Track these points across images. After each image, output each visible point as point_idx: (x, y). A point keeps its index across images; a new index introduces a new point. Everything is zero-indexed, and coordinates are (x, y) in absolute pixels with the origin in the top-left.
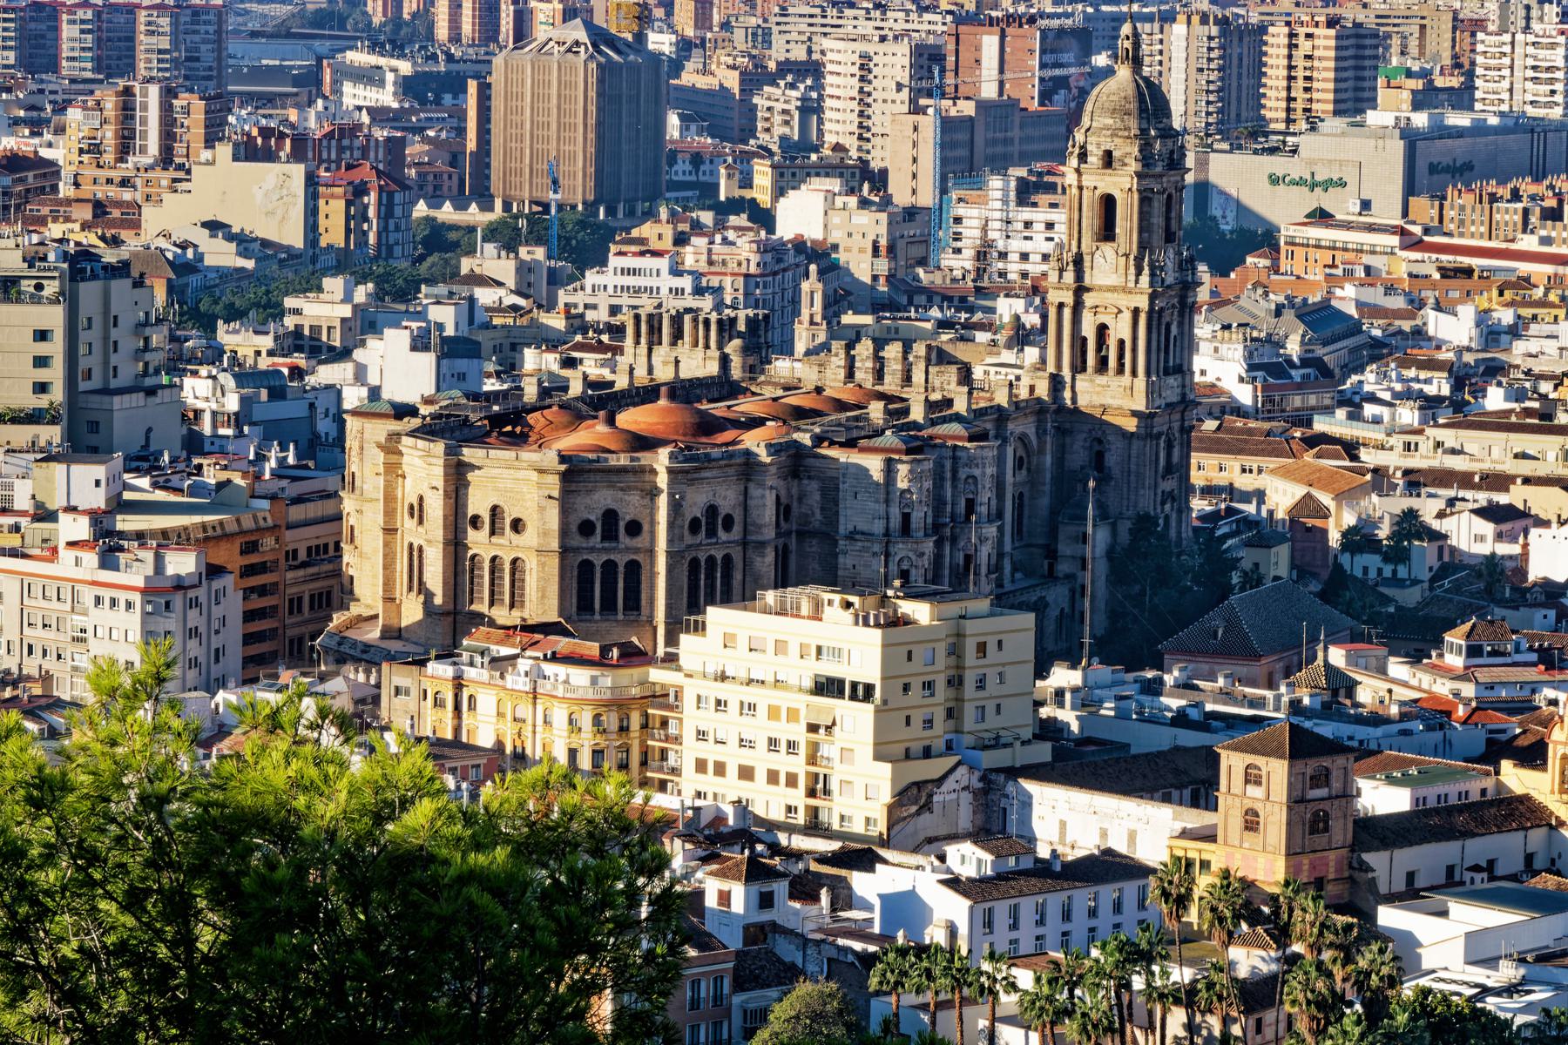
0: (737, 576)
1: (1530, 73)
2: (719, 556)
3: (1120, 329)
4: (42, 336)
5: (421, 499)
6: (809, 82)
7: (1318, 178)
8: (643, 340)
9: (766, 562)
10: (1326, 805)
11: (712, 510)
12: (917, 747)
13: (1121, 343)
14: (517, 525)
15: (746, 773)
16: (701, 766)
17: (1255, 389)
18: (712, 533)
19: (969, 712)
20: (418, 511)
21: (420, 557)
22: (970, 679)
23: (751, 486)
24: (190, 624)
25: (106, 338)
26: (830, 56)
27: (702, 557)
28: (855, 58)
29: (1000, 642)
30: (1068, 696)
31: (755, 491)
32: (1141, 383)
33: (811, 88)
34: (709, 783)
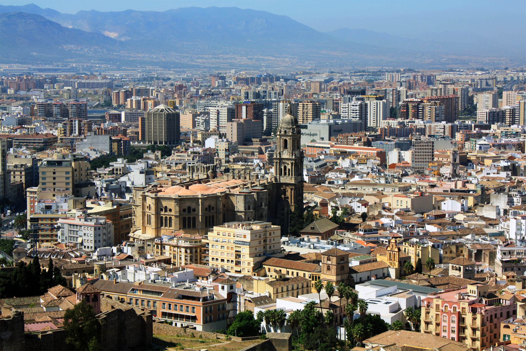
0: (215, 219)
1: (352, 111)
2: (211, 215)
3: (289, 167)
4: (67, 173)
5: (150, 205)
6: (206, 116)
7: (312, 133)
8: (191, 172)
9: (221, 217)
10: (343, 265)
11: (210, 206)
12: (258, 255)
13: (289, 169)
14: (170, 210)
15: (223, 260)
16: (213, 259)
17: (309, 177)
18: (210, 211)
19: (268, 246)
20: (149, 207)
21: (150, 217)
22: (268, 240)
23: (217, 201)
24: (104, 232)
25: (80, 173)
26: (211, 110)
27: (208, 216)
28: (216, 111)
29: (274, 233)
30: (286, 243)
31: (218, 202)
32: (293, 178)
33: (207, 117)
34: (215, 262)
